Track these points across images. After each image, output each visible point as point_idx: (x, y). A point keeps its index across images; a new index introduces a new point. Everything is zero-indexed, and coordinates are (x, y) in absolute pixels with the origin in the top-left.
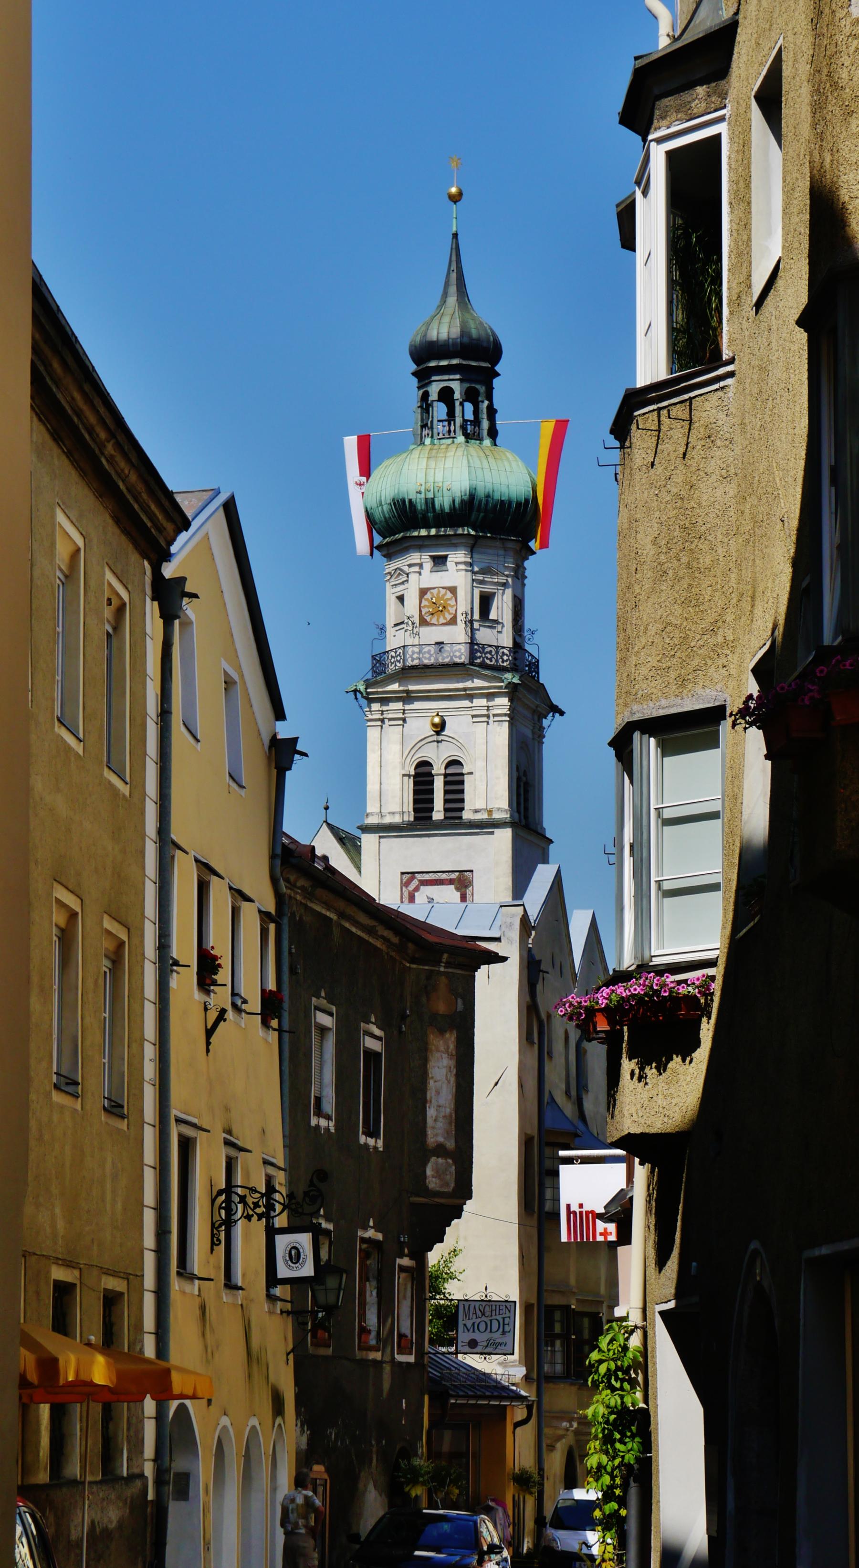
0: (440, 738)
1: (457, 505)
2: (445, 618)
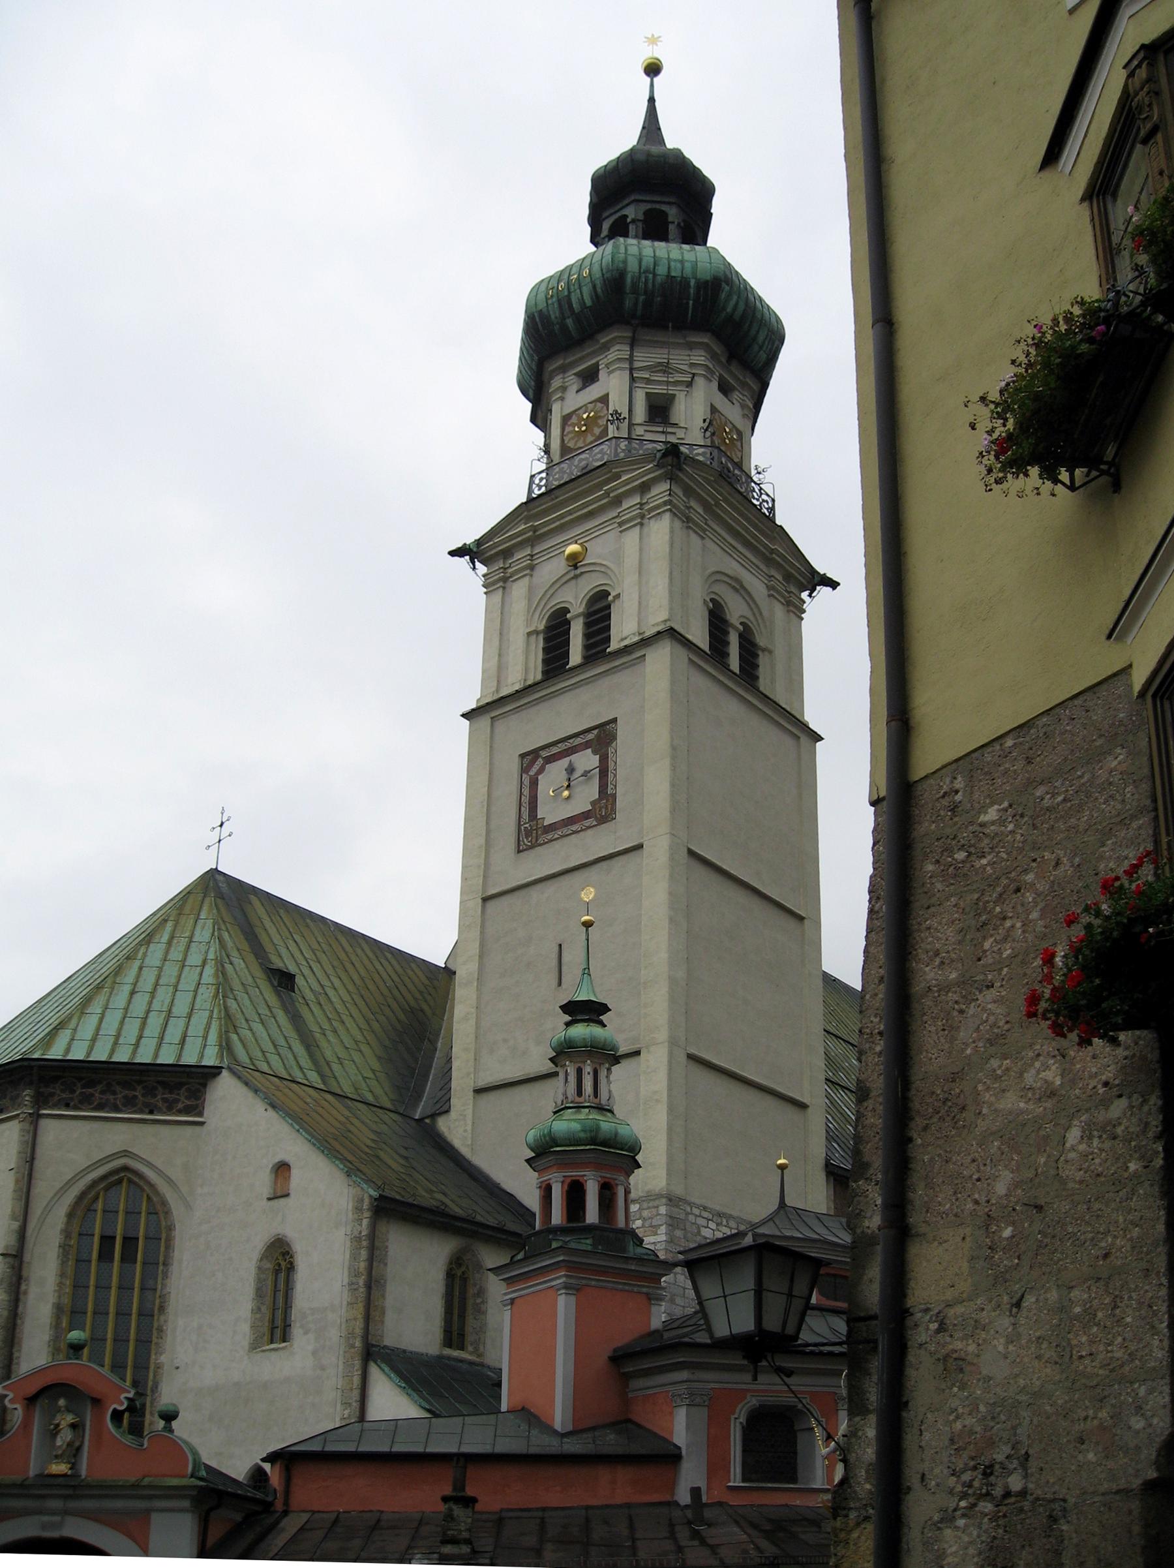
0: (578, 571)
1: (599, 290)
2: (593, 434)
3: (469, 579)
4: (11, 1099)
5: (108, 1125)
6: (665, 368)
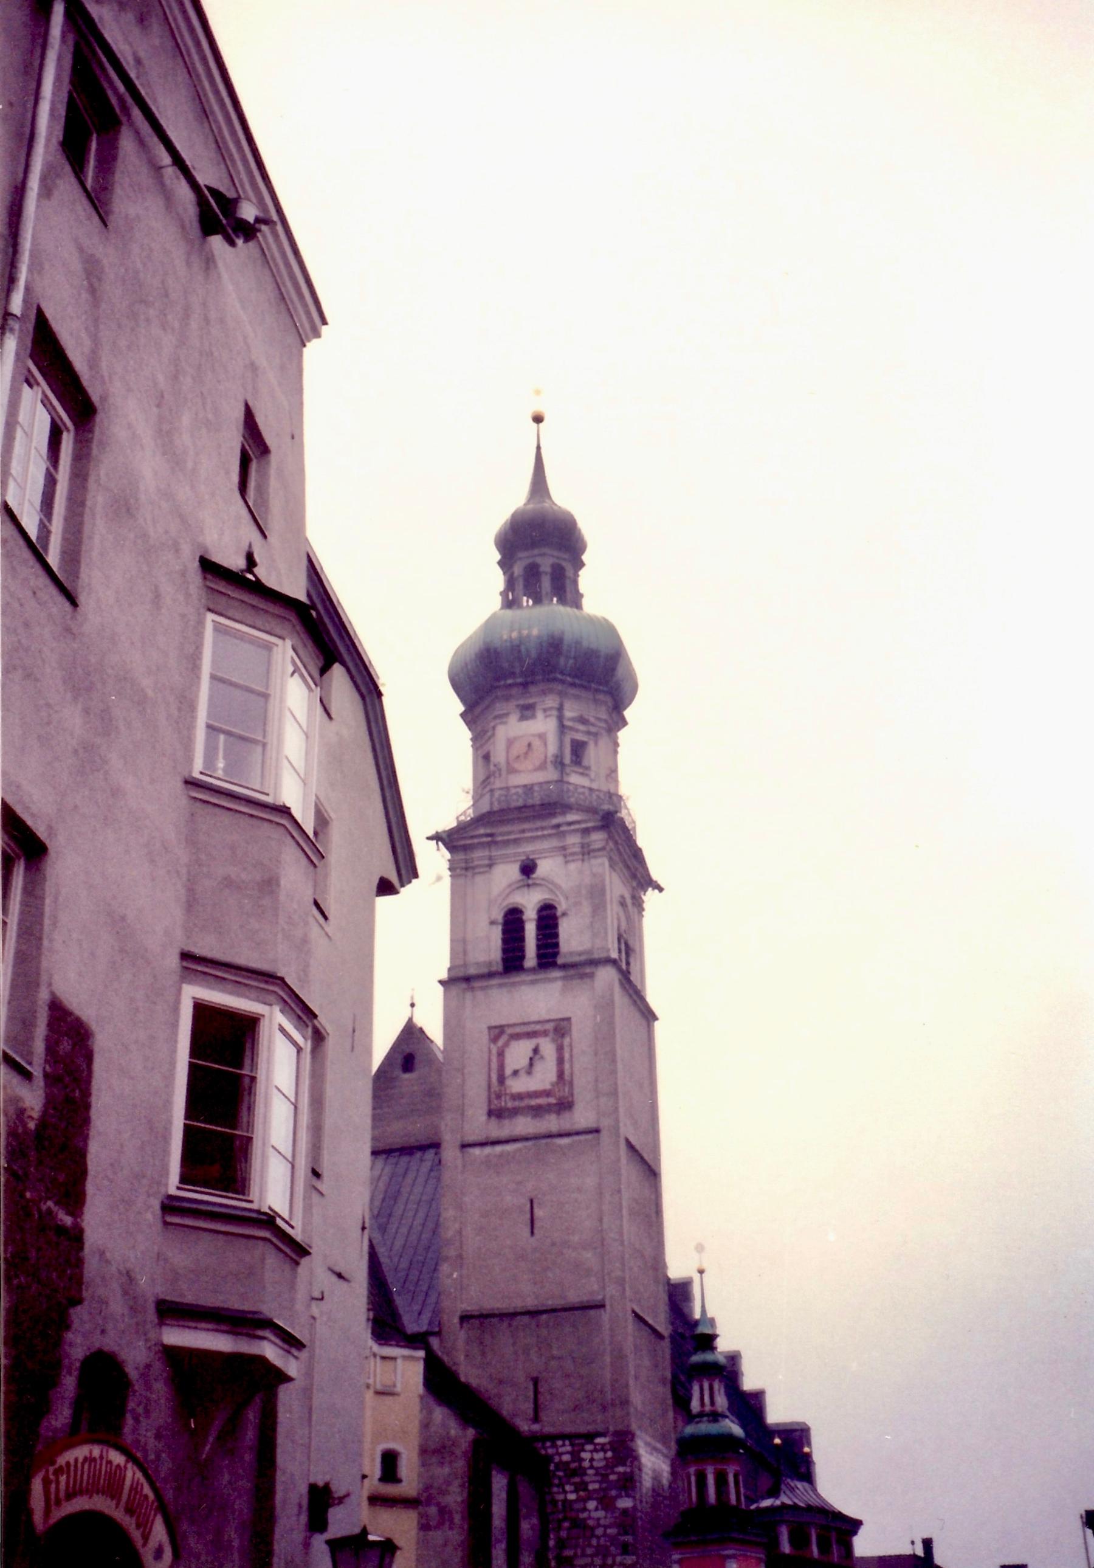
0: (530, 882)
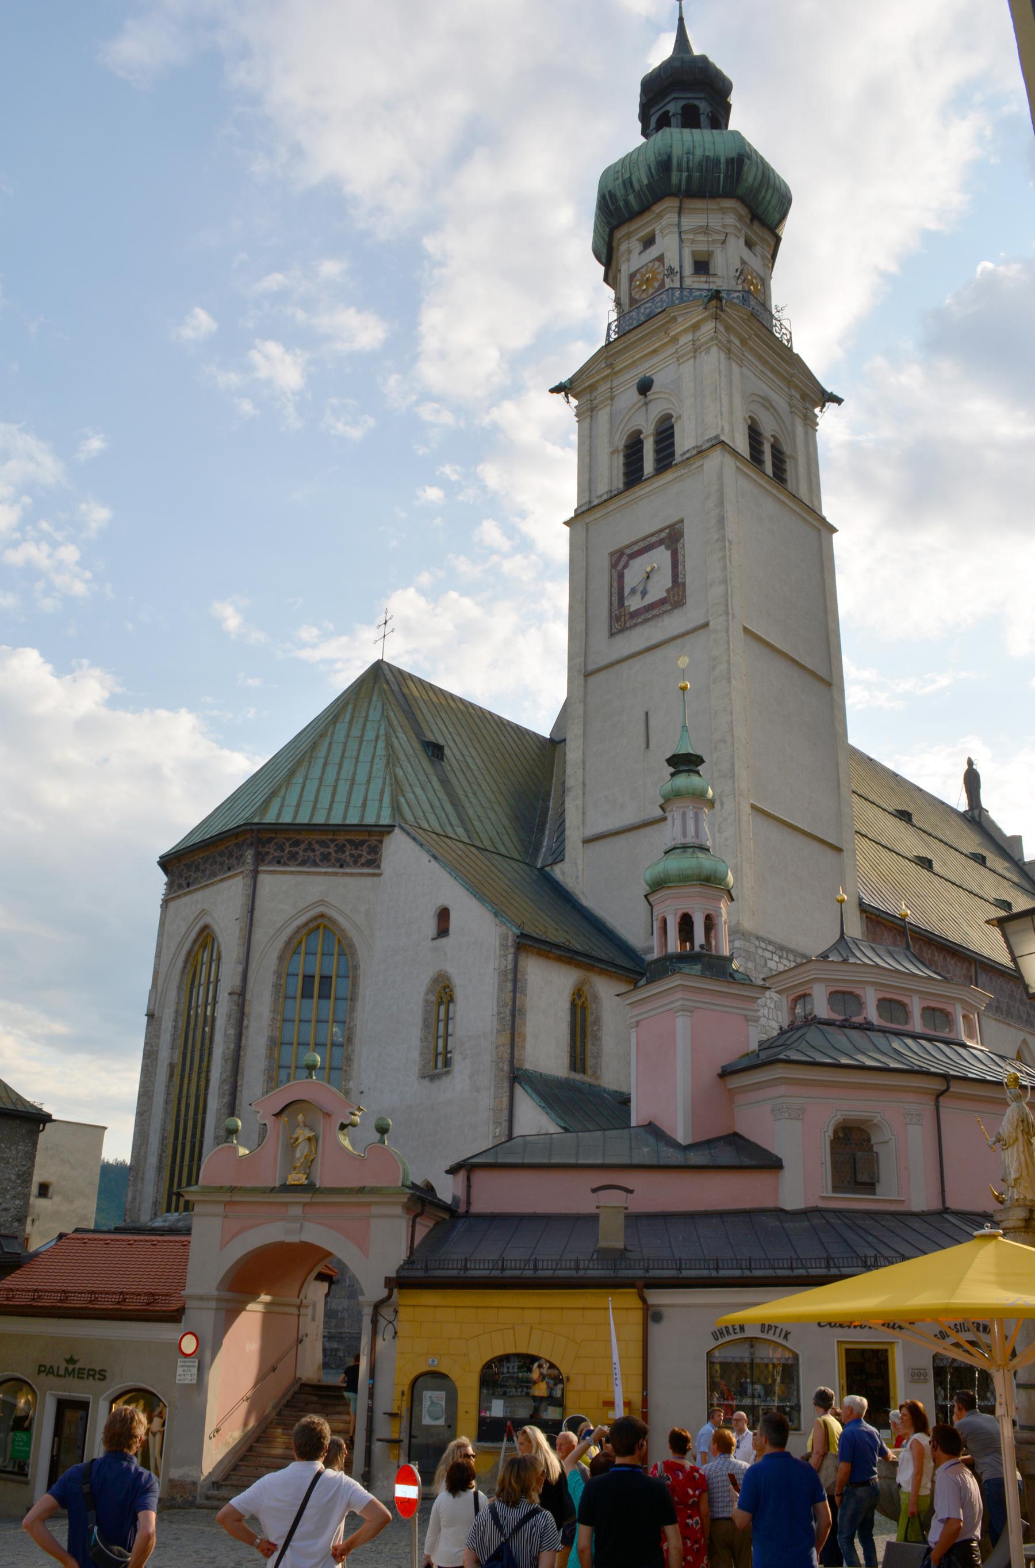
1: (653, 171)
3: (564, 411)
4: (237, 858)
5: (310, 878)
6: (706, 230)
